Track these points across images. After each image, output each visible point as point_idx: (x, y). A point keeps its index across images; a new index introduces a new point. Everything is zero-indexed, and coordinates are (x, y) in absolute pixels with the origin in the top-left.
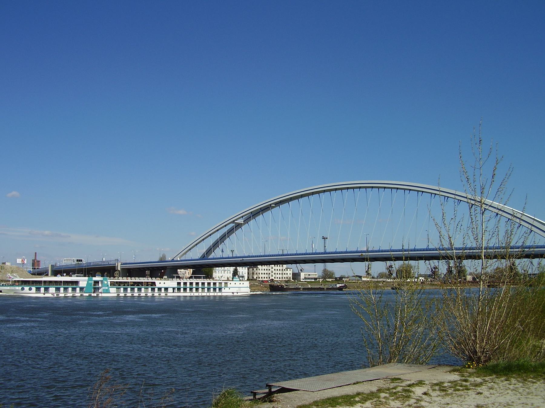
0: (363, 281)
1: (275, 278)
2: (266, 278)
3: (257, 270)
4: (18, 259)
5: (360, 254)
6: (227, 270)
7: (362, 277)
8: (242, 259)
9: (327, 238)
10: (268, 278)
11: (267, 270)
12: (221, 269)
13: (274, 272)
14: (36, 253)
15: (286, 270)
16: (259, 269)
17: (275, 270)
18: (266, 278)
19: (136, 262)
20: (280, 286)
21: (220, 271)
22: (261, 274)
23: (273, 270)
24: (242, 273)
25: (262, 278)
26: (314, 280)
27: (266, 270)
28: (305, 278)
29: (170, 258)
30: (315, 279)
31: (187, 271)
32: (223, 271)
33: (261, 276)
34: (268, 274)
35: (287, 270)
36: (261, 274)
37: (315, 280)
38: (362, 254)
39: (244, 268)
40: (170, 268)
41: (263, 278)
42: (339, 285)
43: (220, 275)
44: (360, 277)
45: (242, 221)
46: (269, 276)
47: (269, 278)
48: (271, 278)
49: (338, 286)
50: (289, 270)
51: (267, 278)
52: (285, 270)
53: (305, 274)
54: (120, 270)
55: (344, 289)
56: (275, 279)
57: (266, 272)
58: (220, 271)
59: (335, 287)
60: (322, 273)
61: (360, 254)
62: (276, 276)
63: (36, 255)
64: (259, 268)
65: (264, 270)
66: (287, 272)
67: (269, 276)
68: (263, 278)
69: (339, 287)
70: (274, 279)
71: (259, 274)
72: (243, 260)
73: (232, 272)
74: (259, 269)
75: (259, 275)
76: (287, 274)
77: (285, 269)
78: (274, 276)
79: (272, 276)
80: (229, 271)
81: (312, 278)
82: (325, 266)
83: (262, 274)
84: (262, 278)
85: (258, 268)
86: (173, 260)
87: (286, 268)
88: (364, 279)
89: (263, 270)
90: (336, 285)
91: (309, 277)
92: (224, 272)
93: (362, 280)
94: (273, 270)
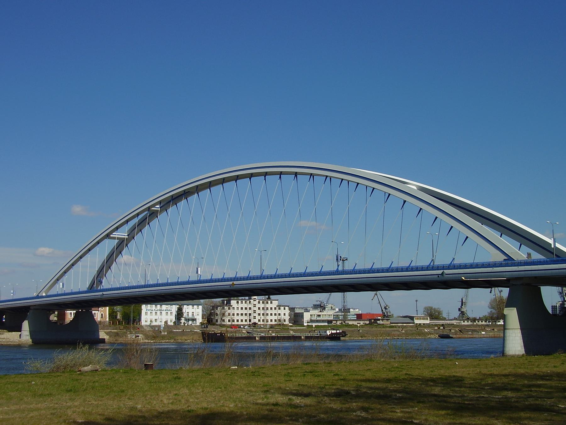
0: (416, 324)
1: (259, 320)
2: (244, 321)
3: (229, 309)
5: (231, 283)
6: (165, 310)
7: (415, 319)
8: (102, 293)
9: (346, 260)
10: (248, 321)
11: (246, 309)
13: (258, 312)
15: (277, 308)
16: (234, 308)
17: (259, 308)
18: (244, 321)
19: (15, 298)
20: (219, 334)
21: (154, 312)
22: (236, 315)
23: (256, 309)
24: (193, 315)
25: (238, 321)
26: (327, 324)
27: (244, 309)
28: (312, 321)
29: (35, 294)
30: (330, 322)
31: (98, 312)
32: (158, 312)
33: (236, 318)
35: (279, 309)
36: (236, 315)
37: (328, 323)
38: (233, 283)
39: (195, 306)
40: (34, 309)
41: (240, 321)
42: (330, 331)
43: (154, 317)
44: (412, 318)
45: (125, 235)
46: (250, 317)
47: (250, 321)
49: (328, 334)
50: (282, 308)
51: (246, 321)
52: (275, 308)
53: (311, 315)
55: (342, 338)
56: (259, 323)
57: (244, 312)
58: (154, 312)
59: (324, 334)
60: (424, 311)
61: (231, 283)
62: (261, 318)
64: (233, 307)
65: (242, 308)
66: (279, 312)
67: (250, 317)
68: (240, 321)
69: (329, 334)
71: (233, 315)
72: (103, 294)
73: (174, 313)
74: (234, 308)
75: (232, 317)
76: (279, 314)
77: (276, 307)
78: (258, 318)
79: (255, 318)
81: (323, 321)
82: (344, 302)
83: (238, 314)
84: (238, 321)
85: (232, 306)
86: (38, 297)
88: (417, 321)
89: (240, 309)
90: (325, 332)
91: (319, 318)
92: (161, 313)
93: (414, 323)
94: (256, 309)
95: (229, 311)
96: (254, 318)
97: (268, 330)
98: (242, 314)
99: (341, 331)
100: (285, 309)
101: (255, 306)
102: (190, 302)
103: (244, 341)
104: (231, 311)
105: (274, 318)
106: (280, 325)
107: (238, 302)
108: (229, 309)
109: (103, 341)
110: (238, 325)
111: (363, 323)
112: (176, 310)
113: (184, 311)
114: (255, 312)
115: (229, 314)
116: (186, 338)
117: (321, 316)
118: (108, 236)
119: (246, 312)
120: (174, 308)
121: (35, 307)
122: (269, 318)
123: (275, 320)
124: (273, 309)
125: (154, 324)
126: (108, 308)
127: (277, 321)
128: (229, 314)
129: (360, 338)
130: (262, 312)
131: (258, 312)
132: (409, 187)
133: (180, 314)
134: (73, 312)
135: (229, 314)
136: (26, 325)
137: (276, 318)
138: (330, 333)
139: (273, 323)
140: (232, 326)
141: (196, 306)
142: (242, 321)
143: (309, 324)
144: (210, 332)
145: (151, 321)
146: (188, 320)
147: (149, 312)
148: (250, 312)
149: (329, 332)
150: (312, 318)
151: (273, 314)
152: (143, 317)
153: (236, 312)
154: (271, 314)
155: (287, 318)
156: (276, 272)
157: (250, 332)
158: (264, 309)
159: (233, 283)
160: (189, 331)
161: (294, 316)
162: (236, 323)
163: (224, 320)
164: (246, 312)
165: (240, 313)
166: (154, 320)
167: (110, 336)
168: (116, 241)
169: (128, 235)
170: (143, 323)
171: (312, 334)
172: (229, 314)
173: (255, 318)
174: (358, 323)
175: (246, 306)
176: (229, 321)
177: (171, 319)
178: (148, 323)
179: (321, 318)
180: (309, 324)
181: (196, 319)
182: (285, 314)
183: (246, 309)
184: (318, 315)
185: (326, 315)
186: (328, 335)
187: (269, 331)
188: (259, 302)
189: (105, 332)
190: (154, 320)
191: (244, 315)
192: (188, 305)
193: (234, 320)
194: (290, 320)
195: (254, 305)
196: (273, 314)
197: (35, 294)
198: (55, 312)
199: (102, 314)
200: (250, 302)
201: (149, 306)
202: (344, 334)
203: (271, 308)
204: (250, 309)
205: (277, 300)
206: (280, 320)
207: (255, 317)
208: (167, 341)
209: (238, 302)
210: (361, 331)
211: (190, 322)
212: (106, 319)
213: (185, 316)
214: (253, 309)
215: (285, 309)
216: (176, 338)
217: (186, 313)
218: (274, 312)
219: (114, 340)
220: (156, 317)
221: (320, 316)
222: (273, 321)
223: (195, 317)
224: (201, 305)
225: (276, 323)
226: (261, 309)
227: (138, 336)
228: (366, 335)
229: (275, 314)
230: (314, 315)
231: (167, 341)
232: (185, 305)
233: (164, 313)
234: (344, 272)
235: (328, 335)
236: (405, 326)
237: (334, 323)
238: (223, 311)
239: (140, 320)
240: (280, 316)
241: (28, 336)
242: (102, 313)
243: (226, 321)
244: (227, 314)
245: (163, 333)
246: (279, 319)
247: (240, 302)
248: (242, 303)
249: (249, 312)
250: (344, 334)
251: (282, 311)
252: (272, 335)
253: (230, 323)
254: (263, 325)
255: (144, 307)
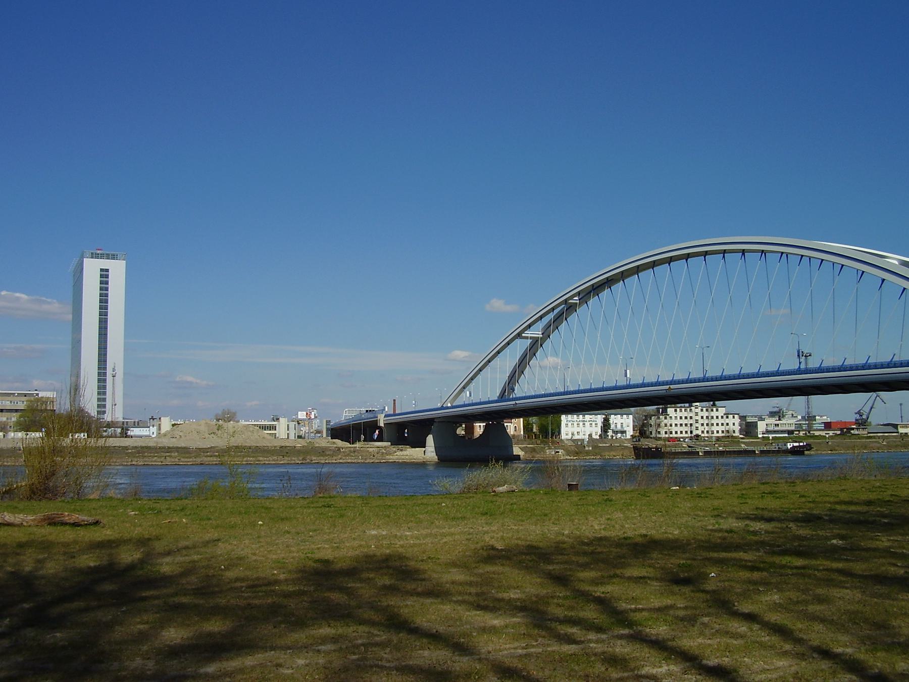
0: (901, 433)
1: (703, 432)
2: (684, 432)
3: (666, 418)
4: (299, 412)
5: (667, 387)
6: (589, 421)
8: (515, 402)
9: (810, 355)
10: (689, 432)
12: (578, 420)
13: (701, 421)
14: (394, 400)
15: (725, 417)
16: (671, 417)
17: (702, 417)
18: (684, 432)
20: (653, 448)
21: (575, 424)
22: (673, 425)
23: (698, 418)
24: (622, 426)
25: (676, 433)
26: (787, 435)
27: (683, 418)
28: (768, 432)
29: (439, 404)
30: (790, 432)
31: (510, 424)
32: (581, 424)
33: (674, 429)
34: (689, 425)
35: (727, 417)
36: (673, 425)
37: (788, 434)
38: (670, 387)
39: (625, 416)
41: (679, 432)
42: (792, 444)
43: (576, 430)
44: (895, 426)
45: (539, 334)
46: (691, 428)
47: (691, 432)
48: (694, 433)
49: (789, 447)
51: (686, 432)
52: (722, 417)
53: (767, 425)
54: (383, 426)
55: (806, 452)
56: (703, 435)
57: (684, 421)
58: (575, 424)
59: (784, 448)
61: (667, 387)
62: (705, 429)
63: (394, 403)
64: (670, 415)
65: (681, 418)
66: (727, 421)
67: (691, 428)
68: (679, 432)
69: (791, 448)
70: (700, 434)
71: (671, 425)
72: (517, 404)
73: (600, 424)
74: (671, 417)
75: (670, 428)
76: (727, 424)
77: (723, 415)
79: (697, 428)
80: (594, 423)
81: (782, 432)
82: (808, 408)
83: (676, 425)
84: (676, 433)
85: (668, 415)
86: (442, 408)
87: (724, 414)
88: (901, 430)
89: (679, 418)
91: (776, 428)
92: (584, 424)
93: (898, 432)
94: (698, 418)
95: (666, 421)
96: (696, 429)
97: (714, 443)
98: (681, 425)
99: (805, 444)
100: (734, 417)
101: (697, 414)
102: (619, 410)
103: (685, 457)
104: (668, 421)
105: (720, 428)
106: (728, 437)
107: (676, 411)
108: (666, 418)
109: (518, 458)
110: (676, 438)
111: (833, 434)
112: (602, 421)
113: (611, 422)
114: (697, 421)
115: (666, 425)
116: (614, 454)
117: (780, 425)
118: (519, 335)
119: (686, 421)
120: (600, 419)
121: (440, 420)
122: (715, 428)
123: (723, 432)
124: (720, 417)
125: (576, 437)
126: (522, 419)
127: (725, 432)
128: (666, 425)
129: (830, 452)
130: (706, 422)
131: (701, 421)
132: (888, 262)
133: (606, 425)
134: (483, 424)
135: (665, 424)
136: (430, 439)
137: (723, 428)
138: (791, 446)
139: (720, 434)
140: (669, 439)
141: (626, 416)
142: (681, 432)
143: (765, 435)
144: (643, 447)
145: (573, 434)
146: (616, 432)
147: (570, 424)
148: (691, 421)
149: (790, 445)
150: (768, 428)
151: (720, 424)
152: (564, 429)
153: (674, 422)
154: (717, 424)
155: (737, 428)
156: (759, 370)
157: (691, 445)
158: (708, 418)
159: (670, 387)
160: (618, 445)
161: (746, 426)
162: (674, 435)
163: (659, 433)
164: (686, 421)
165: (679, 424)
166: (576, 433)
167: (526, 452)
168: (529, 341)
169: (543, 334)
170: (563, 436)
171: (768, 447)
172: (665, 424)
173: (698, 429)
174: (826, 434)
175: (684, 414)
176: (666, 433)
177: (596, 431)
178: (569, 437)
179: (779, 428)
180: (765, 435)
181: (625, 431)
182: (734, 424)
183: (686, 418)
184: (776, 425)
185: (785, 424)
186: (789, 448)
187: (714, 445)
188: (702, 410)
189: (519, 447)
190: (576, 433)
191: (684, 425)
192: (615, 415)
193: (672, 432)
194: (741, 431)
195: (696, 413)
196: (720, 424)
197: (439, 405)
198: (462, 425)
199: (515, 427)
200: (691, 410)
201: (569, 416)
202: (809, 447)
203: (717, 417)
204: (691, 418)
205: (724, 407)
206: (728, 431)
207: (698, 427)
208: (593, 457)
209: (676, 411)
210: (830, 443)
211: (619, 435)
212: (520, 431)
213: (613, 427)
214: (695, 418)
215: (734, 417)
216: (603, 454)
217: (614, 424)
218: (720, 421)
219: (531, 456)
220: (579, 430)
221: (778, 425)
222: (720, 432)
223: (625, 429)
224: (630, 414)
225: (723, 435)
226: (705, 418)
227: (558, 452)
228: (837, 448)
229: (722, 424)
230: (771, 424)
231: (593, 457)
232: (613, 414)
233: (587, 424)
234: (807, 371)
235: (789, 448)
236: (887, 436)
237: (796, 434)
238: (658, 420)
239: (559, 433)
240: (728, 427)
241: (433, 452)
242: (516, 425)
243: (662, 434)
244: (663, 424)
245: (587, 448)
246: (727, 429)
247: (678, 409)
248: (681, 411)
249: (689, 422)
250: (809, 447)
251: (730, 420)
252: (718, 449)
253: (667, 436)
254: (707, 437)
255: (563, 417)
